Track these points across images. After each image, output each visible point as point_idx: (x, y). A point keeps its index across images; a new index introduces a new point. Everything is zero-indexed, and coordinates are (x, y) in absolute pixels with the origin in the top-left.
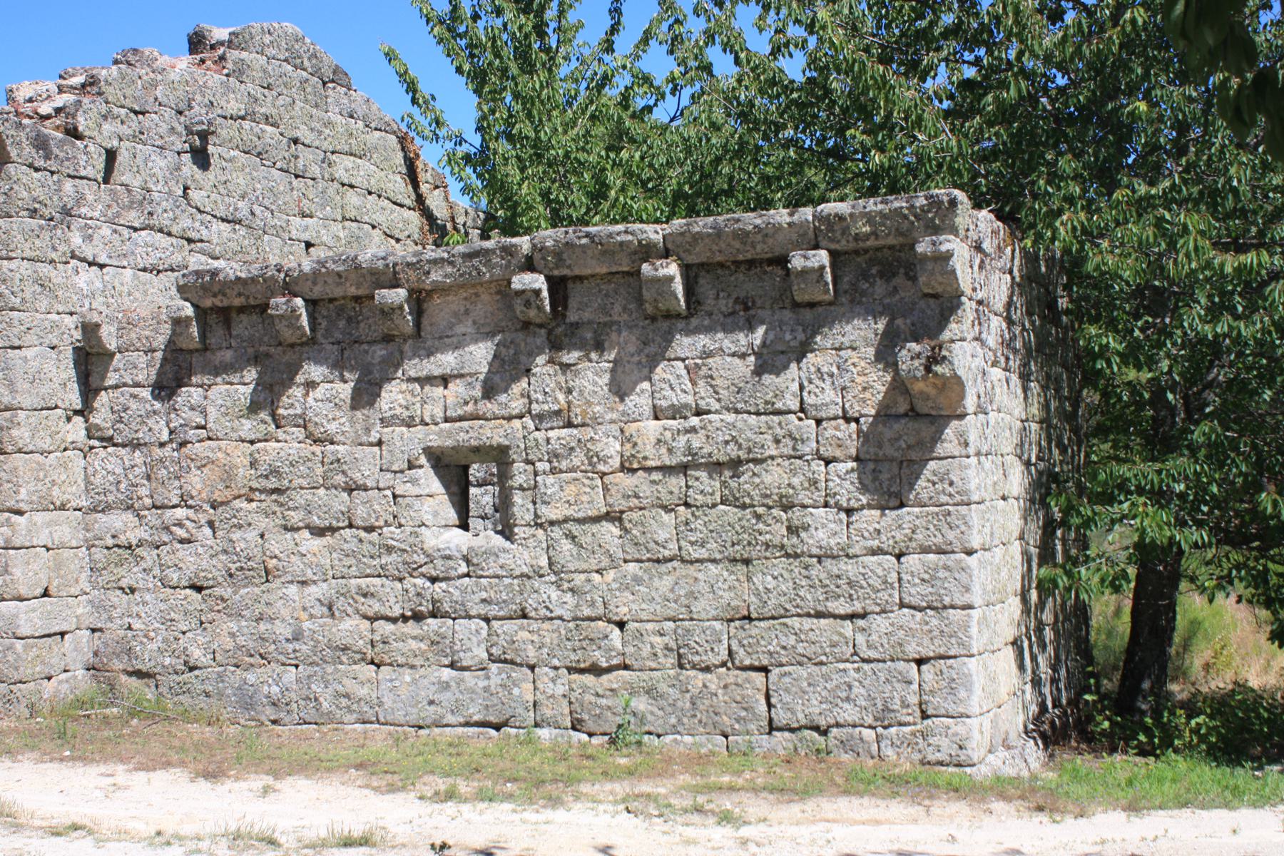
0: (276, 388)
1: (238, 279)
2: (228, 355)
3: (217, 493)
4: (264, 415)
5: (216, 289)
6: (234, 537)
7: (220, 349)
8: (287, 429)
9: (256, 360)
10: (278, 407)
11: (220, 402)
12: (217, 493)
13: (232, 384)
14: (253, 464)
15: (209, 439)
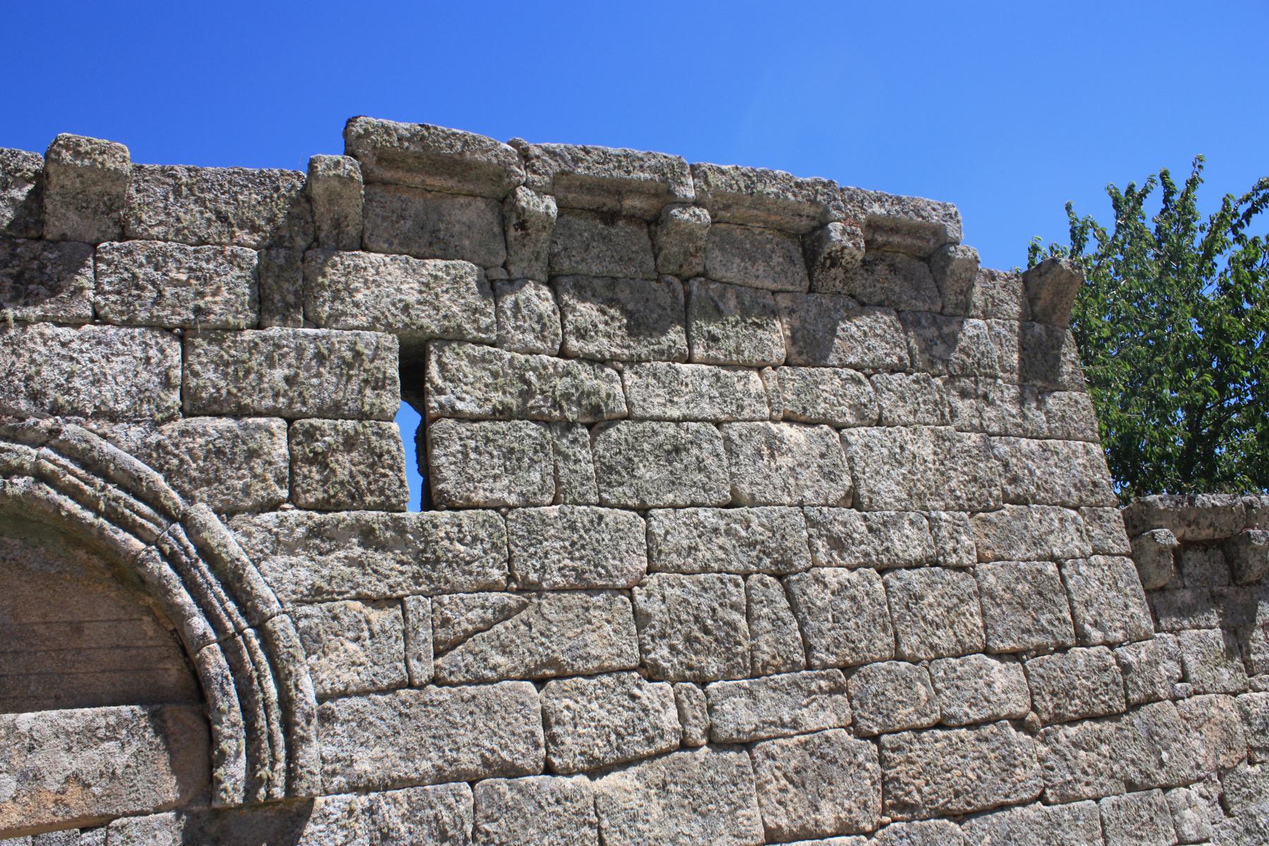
0: (1241, 631)
1: (1214, 506)
2: (1186, 596)
3: (1222, 758)
4: (1237, 661)
5: (1192, 517)
6: (1253, 808)
7: (1178, 588)
8: (1260, 676)
9: (1215, 599)
10: (1249, 652)
11: (1195, 648)
12: (1222, 758)
13: (1199, 627)
14: (1246, 718)
15: (1196, 693)
